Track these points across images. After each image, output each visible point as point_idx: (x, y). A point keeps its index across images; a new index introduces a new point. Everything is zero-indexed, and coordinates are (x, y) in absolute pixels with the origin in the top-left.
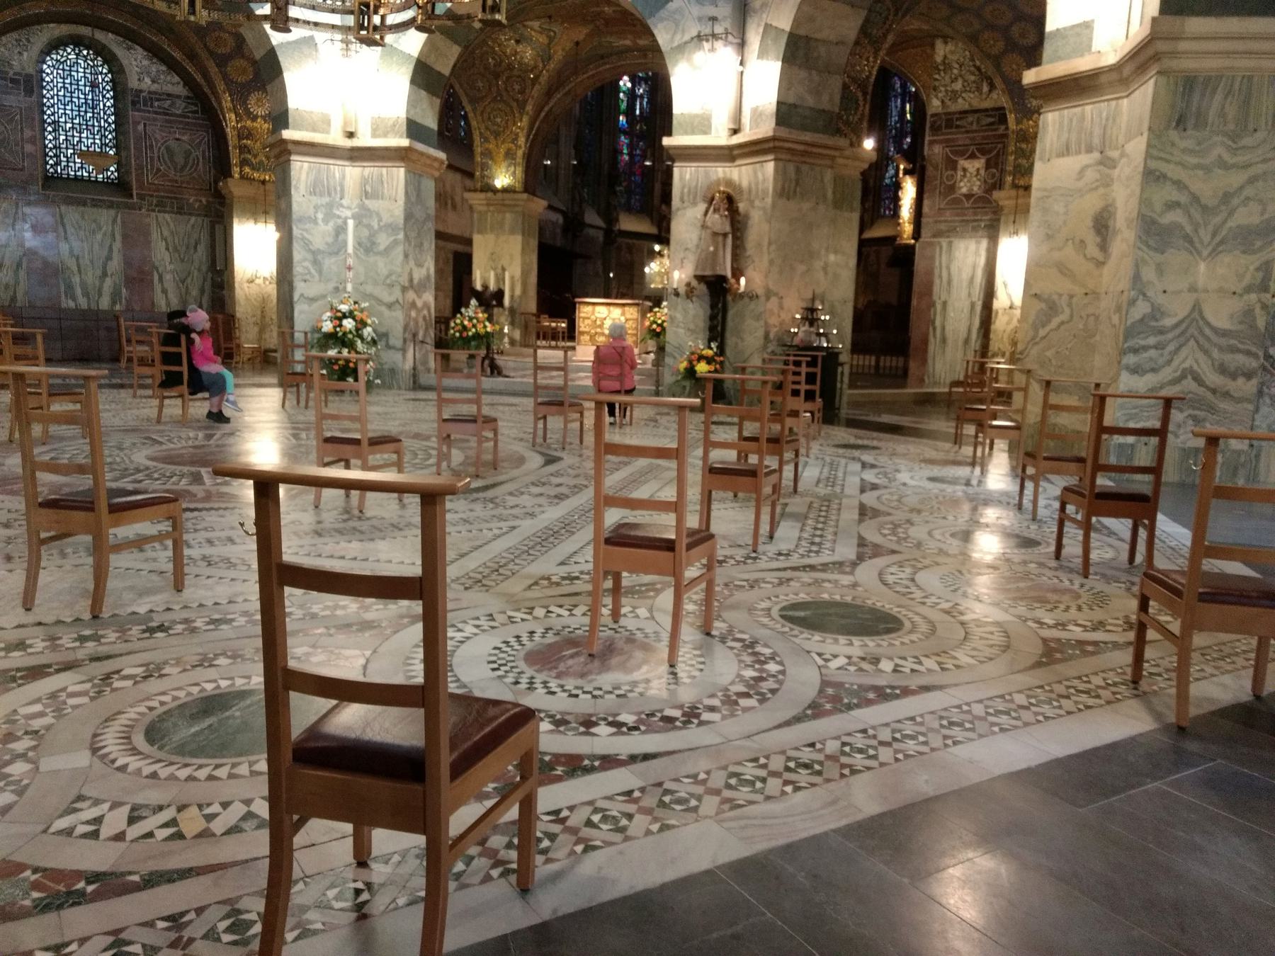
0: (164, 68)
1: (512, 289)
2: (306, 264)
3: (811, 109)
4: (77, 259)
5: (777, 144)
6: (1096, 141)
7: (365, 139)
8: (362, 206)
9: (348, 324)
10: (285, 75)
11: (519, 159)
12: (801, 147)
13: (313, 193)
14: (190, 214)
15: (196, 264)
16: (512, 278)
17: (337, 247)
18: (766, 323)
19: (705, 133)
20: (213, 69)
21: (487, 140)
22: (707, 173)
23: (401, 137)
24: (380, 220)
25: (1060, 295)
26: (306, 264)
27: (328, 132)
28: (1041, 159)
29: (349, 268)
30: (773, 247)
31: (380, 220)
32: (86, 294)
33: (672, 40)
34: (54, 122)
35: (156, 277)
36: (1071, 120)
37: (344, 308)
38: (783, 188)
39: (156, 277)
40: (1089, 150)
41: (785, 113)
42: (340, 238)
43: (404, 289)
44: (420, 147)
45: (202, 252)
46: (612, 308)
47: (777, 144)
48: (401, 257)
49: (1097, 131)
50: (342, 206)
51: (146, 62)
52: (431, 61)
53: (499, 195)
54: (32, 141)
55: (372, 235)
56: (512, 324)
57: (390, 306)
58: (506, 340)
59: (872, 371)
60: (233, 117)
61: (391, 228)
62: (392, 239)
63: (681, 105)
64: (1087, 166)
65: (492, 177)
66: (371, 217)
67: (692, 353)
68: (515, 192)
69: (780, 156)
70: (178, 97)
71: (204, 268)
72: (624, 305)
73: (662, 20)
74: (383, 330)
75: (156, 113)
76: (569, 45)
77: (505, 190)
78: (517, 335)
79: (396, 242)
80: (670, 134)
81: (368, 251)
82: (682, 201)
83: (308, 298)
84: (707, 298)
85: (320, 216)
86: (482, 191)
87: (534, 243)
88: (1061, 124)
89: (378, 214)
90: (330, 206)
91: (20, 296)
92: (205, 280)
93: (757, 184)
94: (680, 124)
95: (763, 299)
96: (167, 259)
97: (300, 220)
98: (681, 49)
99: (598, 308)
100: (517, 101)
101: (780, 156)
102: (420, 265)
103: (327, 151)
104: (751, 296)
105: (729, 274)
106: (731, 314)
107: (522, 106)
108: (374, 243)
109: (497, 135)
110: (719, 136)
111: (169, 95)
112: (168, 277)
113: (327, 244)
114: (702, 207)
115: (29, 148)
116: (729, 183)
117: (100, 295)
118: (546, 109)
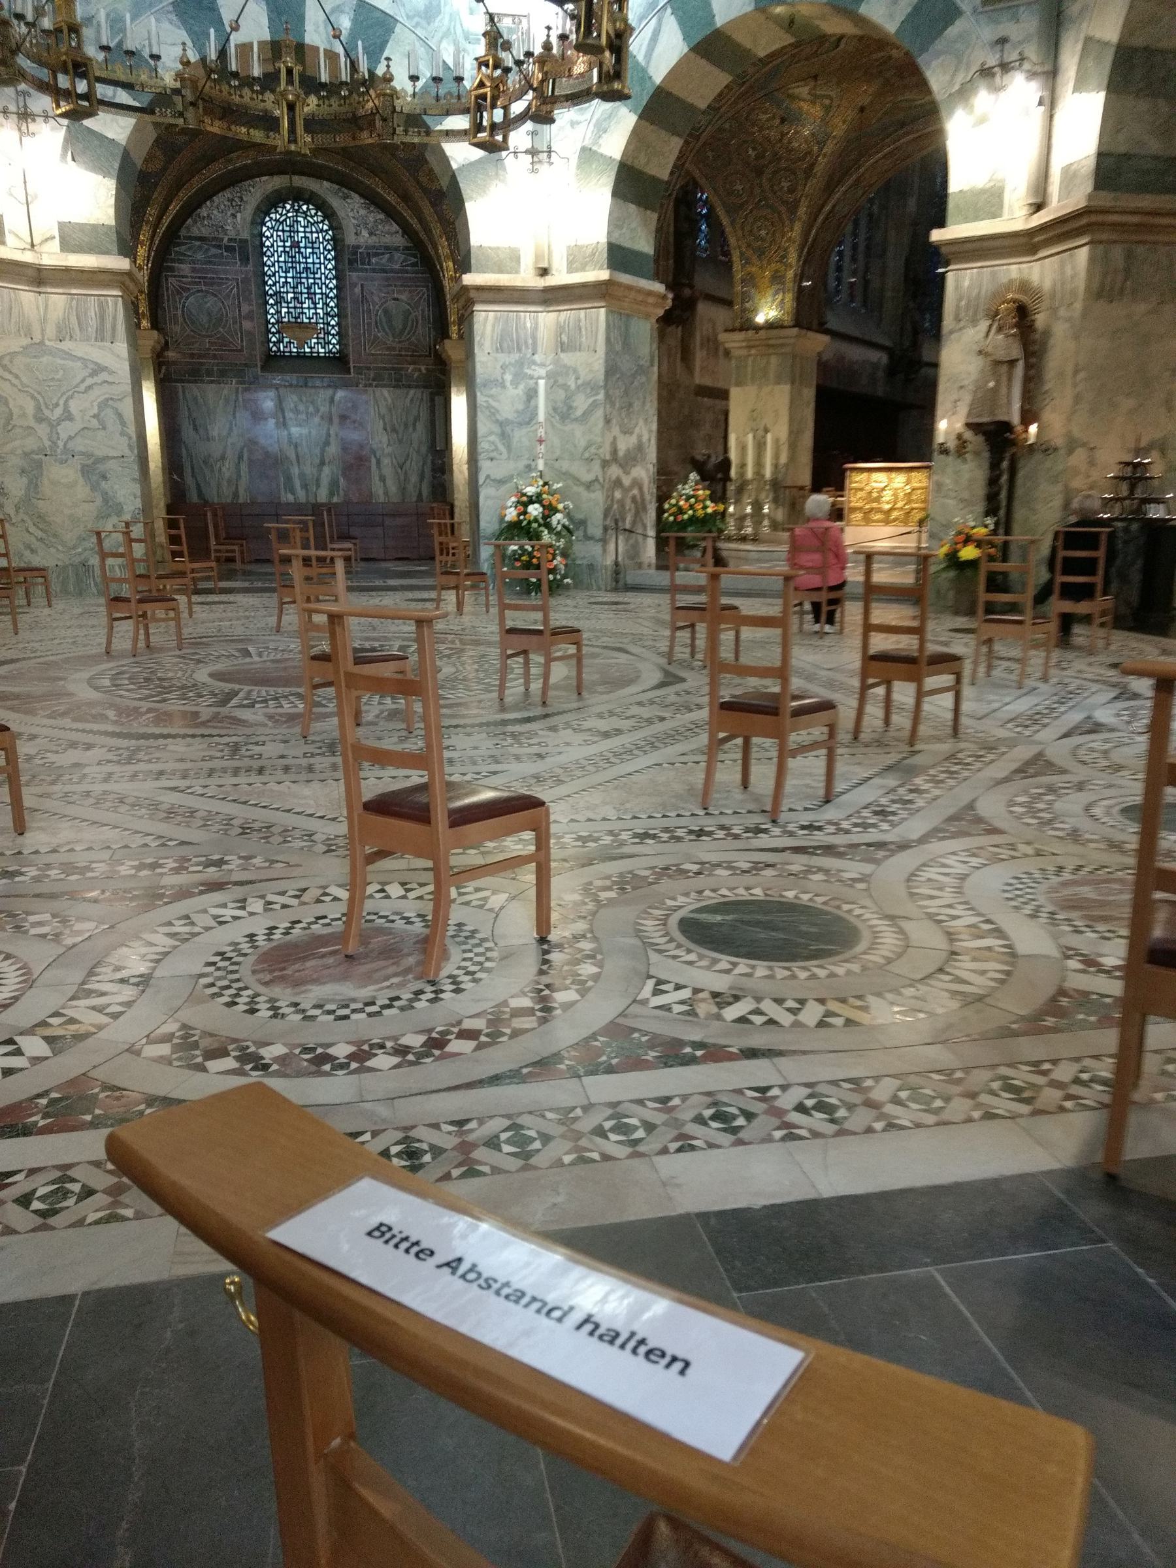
0: (382, 216)
1: (776, 456)
2: (492, 438)
3: (1156, 158)
4: (296, 446)
5: (1094, 218)
7: (561, 277)
8: (556, 362)
9: (535, 510)
10: (469, 206)
11: (789, 284)
12: (1135, 219)
13: (500, 349)
14: (409, 387)
15: (415, 445)
16: (777, 441)
17: (528, 417)
18: (1066, 486)
19: (995, 214)
20: (428, 211)
21: (748, 262)
22: (994, 274)
23: (601, 268)
24: (577, 378)
27: (517, 272)
29: (541, 441)
30: (1082, 375)
32: (305, 486)
33: (951, 82)
34: (276, 293)
35: (374, 461)
37: (531, 490)
38: (1102, 284)
39: (374, 461)
41: (1110, 168)
42: (533, 403)
43: (605, 464)
44: (625, 278)
45: (420, 433)
46: (893, 475)
47: (1094, 218)
48: (601, 423)
50: (534, 363)
51: (363, 212)
52: (641, 163)
53: (762, 332)
54: (250, 316)
55: (568, 398)
56: (776, 501)
57: (589, 486)
58: (766, 522)
60: (450, 264)
61: (589, 387)
63: (962, 177)
65: (755, 311)
66: (567, 374)
67: (959, 533)
68: (782, 327)
69: (1104, 237)
70: (397, 249)
71: (424, 449)
73: (938, 54)
74: (579, 516)
75: (374, 270)
76: (851, 114)
77: (770, 326)
78: (780, 515)
79: (594, 405)
80: (941, 223)
82: (958, 319)
84: (987, 455)
85: (508, 377)
86: (741, 330)
87: (809, 394)
89: (575, 371)
90: (520, 364)
91: (241, 492)
93: (1063, 284)
94: (957, 206)
95: (1062, 452)
96: (385, 439)
98: (964, 93)
99: (876, 476)
100: (784, 202)
101: (1098, 237)
102: (627, 432)
103: (516, 295)
104: (1043, 448)
105: (1016, 419)
106: (1021, 475)
107: (793, 208)
108: (570, 408)
109: (761, 253)
110: (1015, 218)
111: (387, 248)
112: (386, 461)
113: (517, 412)
114: (984, 325)
115: (247, 325)
116: (1024, 286)
117: (318, 486)
118: (827, 208)
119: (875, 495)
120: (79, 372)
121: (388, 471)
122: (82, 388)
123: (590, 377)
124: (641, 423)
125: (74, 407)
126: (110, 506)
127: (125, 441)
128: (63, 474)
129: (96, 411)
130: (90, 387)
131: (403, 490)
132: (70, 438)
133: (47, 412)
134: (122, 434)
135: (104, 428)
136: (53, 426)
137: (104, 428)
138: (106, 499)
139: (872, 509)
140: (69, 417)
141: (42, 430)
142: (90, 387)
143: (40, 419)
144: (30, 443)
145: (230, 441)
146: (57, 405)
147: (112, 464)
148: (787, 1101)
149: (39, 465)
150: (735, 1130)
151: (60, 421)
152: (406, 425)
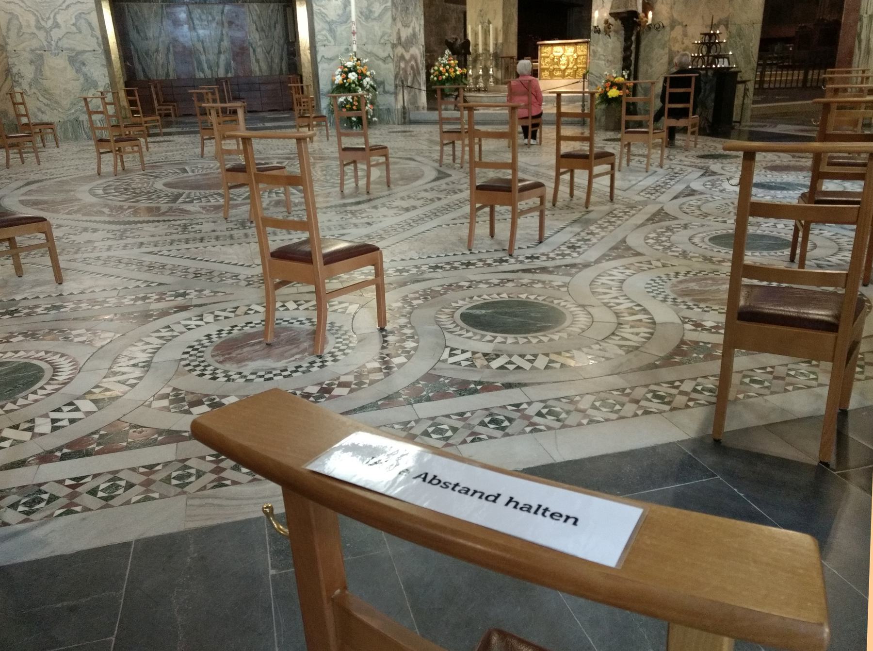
1: (496, 39)
2: (324, 32)
4: (202, 42)
9: (353, 76)
15: (276, 39)
16: (496, 29)
17: (345, 18)
18: (670, 50)
29: (354, 33)
32: (210, 68)
37: (350, 64)
39: (251, 50)
42: (347, 10)
43: (394, 46)
45: (279, 31)
46: (566, 47)
48: (390, 21)
56: (496, 66)
57: (384, 60)
58: (491, 80)
59: (800, 85)
62: (383, 7)
67: (607, 81)
71: (282, 42)
72: (576, 44)
74: (379, 79)
78: (499, 75)
79: (386, 9)
81: (367, 18)
83: (327, 59)
84: (623, 32)
91: (171, 73)
92: (283, 50)
95: (668, 29)
96: (257, 36)
99: (556, 48)
102: (406, 26)
104: (657, 27)
105: (640, 9)
106: (643, 44)
108: (371, 11)
112: (259, 50)
117: (218, 66)
119: (556, 60)
121: (261, 56)
122: (64, 6)
124: (414, 19)
126: (90, 83)
127: (95, 40)
128: (57, 63)
129: (73, 21)
131: (271, 68)
132: (60, 39)
133: (43, 23)
136: (48, 32)
137: (80, 32)
138: (86, 80)
139: (554, 69)
140: (57, 25)
141: (41, 35)
143: (39, 28)
144: (35, 44)
145: (161, 39)
146: (49, 18)
148: (532, 411)
149: (41, 56)
150: (503, 429)
151: (51, 28)
152: (270, 27)
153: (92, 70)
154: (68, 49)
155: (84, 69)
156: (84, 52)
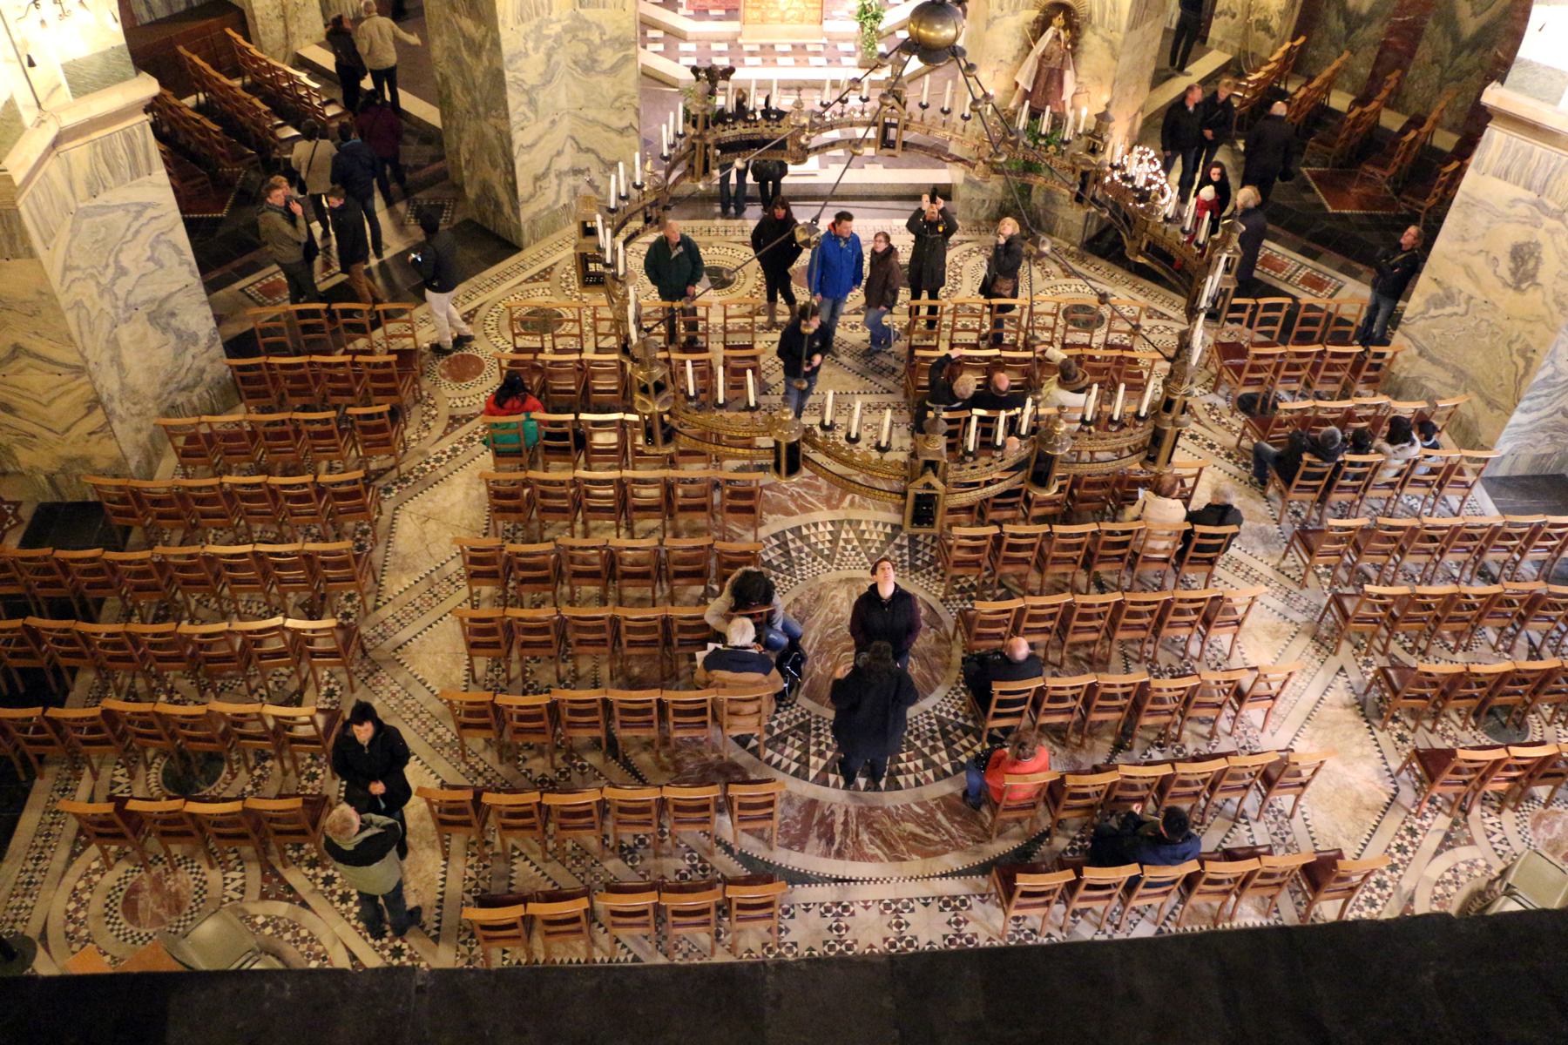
6: (1537, 183)
8: (576, 17)
13: (522, 20)
24: (603, 33)
25: (1460, 292)
26: (523, 108)
28: (1476, 167)
31: (603, 33)
36: (1517, 151)
40: (1528, 187)
42: (555, 58)
49: (1540, 177)
50: (551, 22)
55: (590, 51)
57: (621, 132)
61: (622, 43)
62: (621, 55)
64: (1521, 200)
66: (589, 29)
81: (588, 70)
85: (530, 45)
88: (1507, 148)
89: (599, 26)
90: (539, 28)
97: (510, 61)
108: (595, 61)
120: (120, 219)
122: (129, 236)
123: (618, 33)
125: (125, 260)
126: (186, 339)
127: (185, 267)
129: (149, 253)
130: (137, 232)
132: (129, 293)
134: (181, 264)
135: (162, 267)
137: (162, 267)
140: (122, 272)
142: (137, 232)
146: (107, 265)
147: (180, 299)
151: (113, 281)
153: (187, 318)
154: (144, 303)
155: (174, 322)
156: (171, 295)
